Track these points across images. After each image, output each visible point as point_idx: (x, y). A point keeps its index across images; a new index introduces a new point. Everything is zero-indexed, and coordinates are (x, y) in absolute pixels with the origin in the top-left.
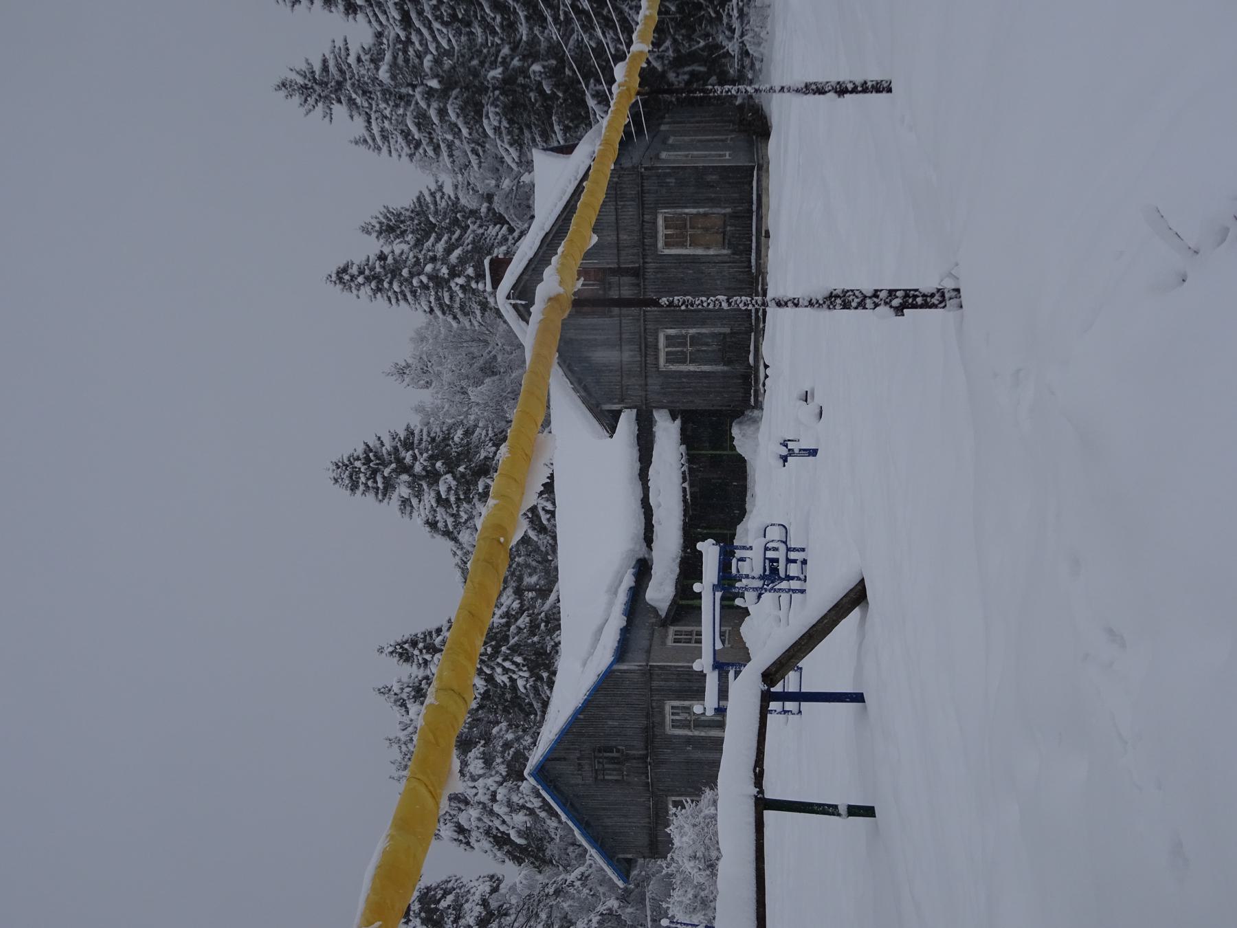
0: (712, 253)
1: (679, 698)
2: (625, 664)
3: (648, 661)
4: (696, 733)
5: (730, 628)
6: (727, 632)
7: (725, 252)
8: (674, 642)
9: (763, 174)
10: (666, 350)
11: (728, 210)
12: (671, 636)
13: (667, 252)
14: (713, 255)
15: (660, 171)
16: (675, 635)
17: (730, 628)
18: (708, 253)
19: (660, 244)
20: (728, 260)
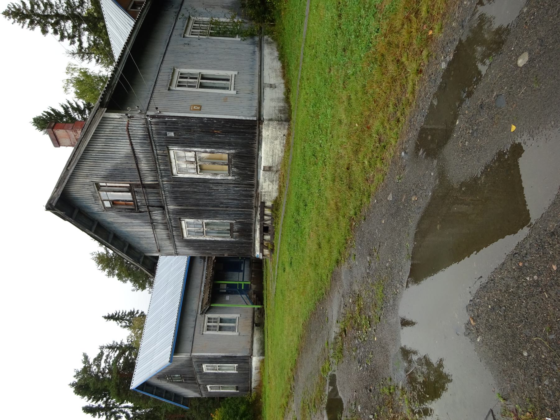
0: (219, 178)
1: (208, 363)
2: (178, 354)
3: (192, 352)
4: (220, 372)
5: (239, 315)
6: (237, 319)
7: (230, 178)
8: (208, 330)
9: (263, 127)
10: (187, 229)
11: (233, 151)
12: (206, 324)
13: (180, 175)
14: (219, 179)
15: (167, 119)
16: (209, 322)
17: (239, 315)
18: (216, 178)
19: (175, 171)
20: (233, 183)
